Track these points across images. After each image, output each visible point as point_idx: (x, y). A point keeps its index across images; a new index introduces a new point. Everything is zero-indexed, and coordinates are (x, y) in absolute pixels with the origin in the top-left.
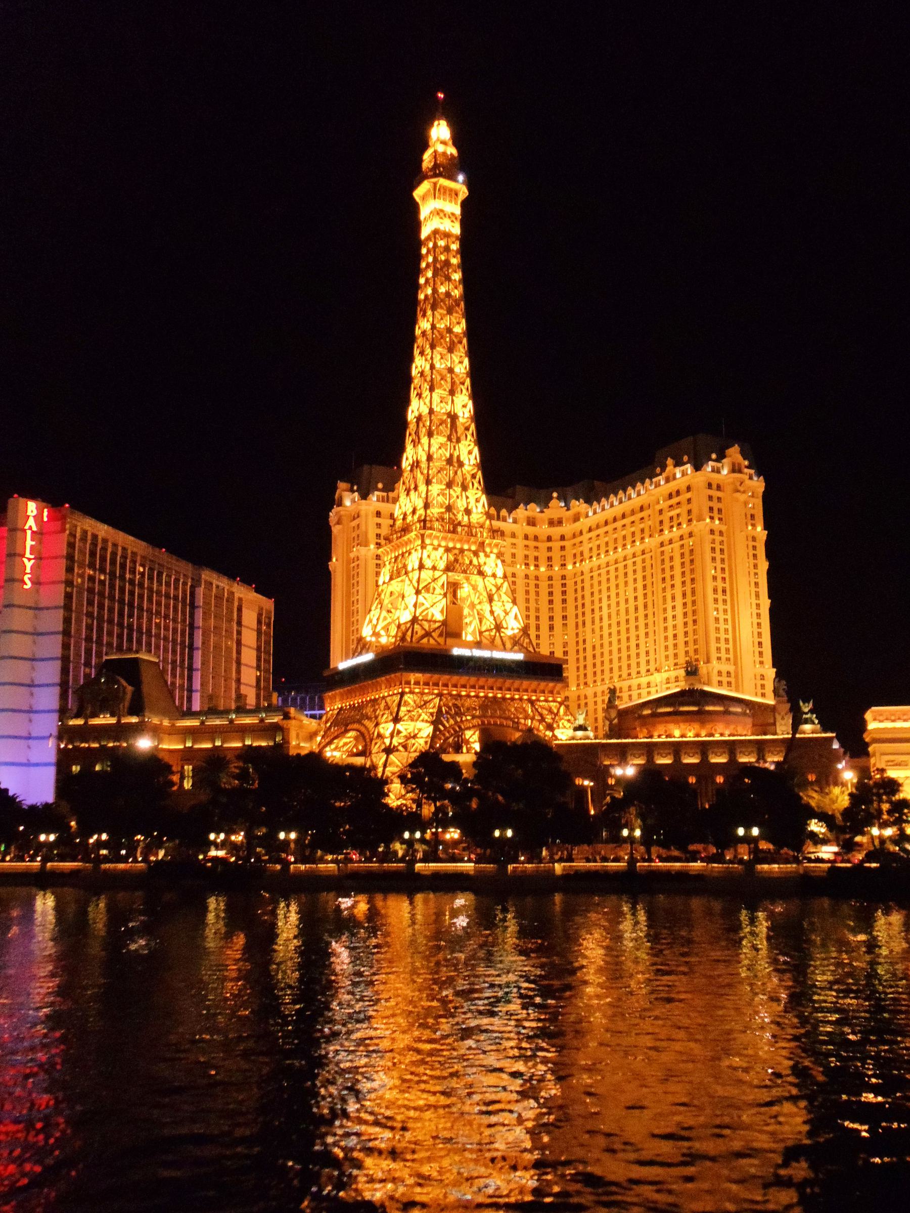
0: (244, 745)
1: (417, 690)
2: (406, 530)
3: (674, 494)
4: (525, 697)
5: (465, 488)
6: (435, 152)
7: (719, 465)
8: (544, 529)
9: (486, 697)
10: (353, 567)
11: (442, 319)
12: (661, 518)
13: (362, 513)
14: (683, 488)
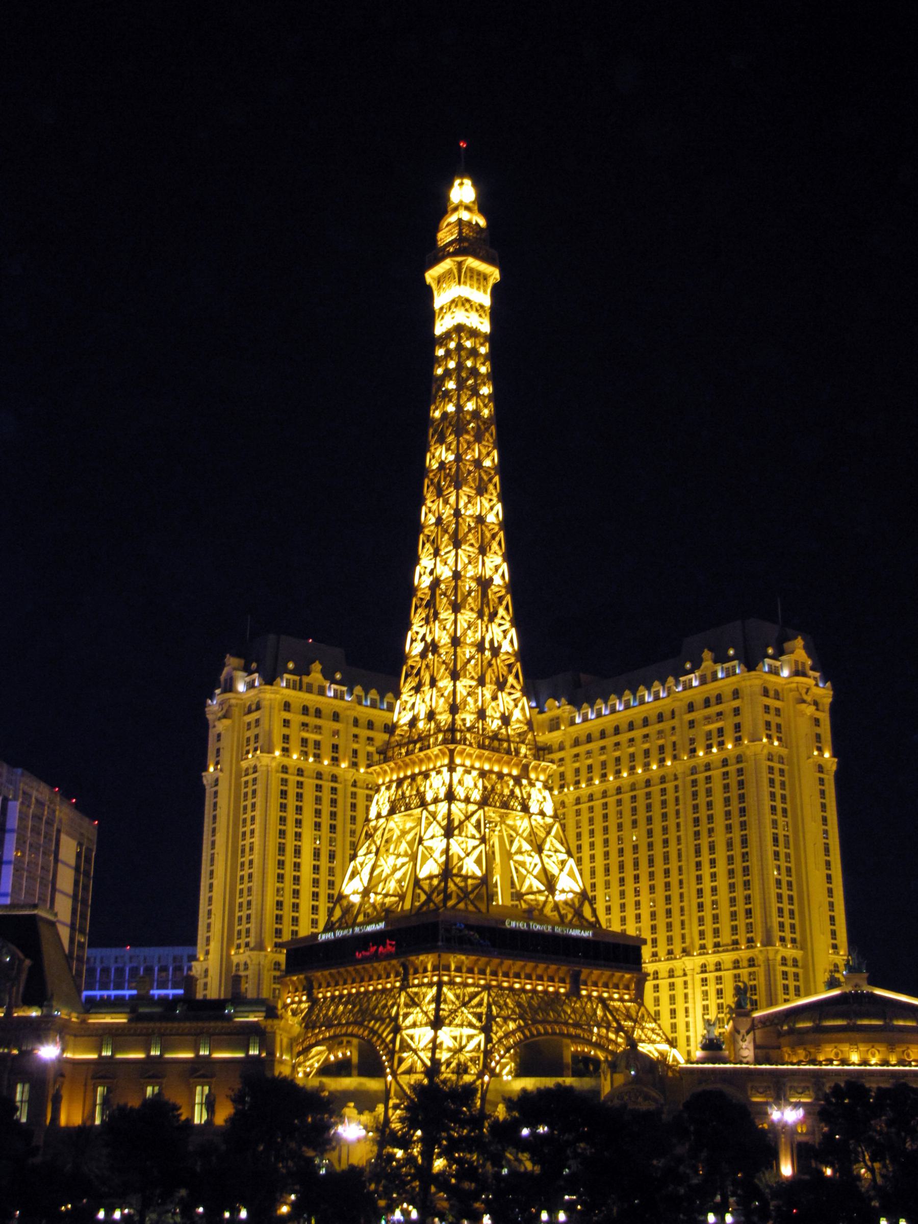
0: (198, 1056)
1: (458, 980)
2: (422, 741)
3: (713, 700)
4: (595, 994)
5: (501, 685)
6: (460, 220)
7: (778, 664)
9: (534, 991)
10: (246, 786)
11: (469, 448)
12: (692, 733)
13: (265, 703)
14: (727, 692)
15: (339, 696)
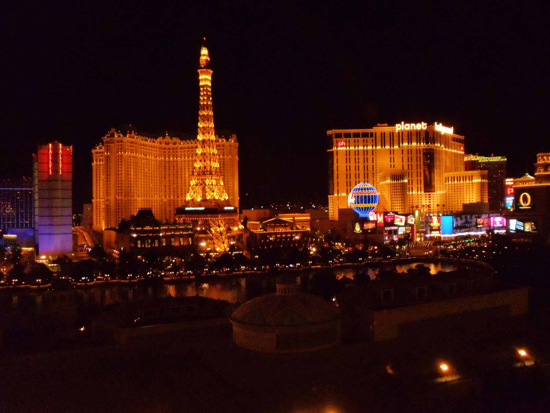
8: (163, 145)
15: (137, 138)
